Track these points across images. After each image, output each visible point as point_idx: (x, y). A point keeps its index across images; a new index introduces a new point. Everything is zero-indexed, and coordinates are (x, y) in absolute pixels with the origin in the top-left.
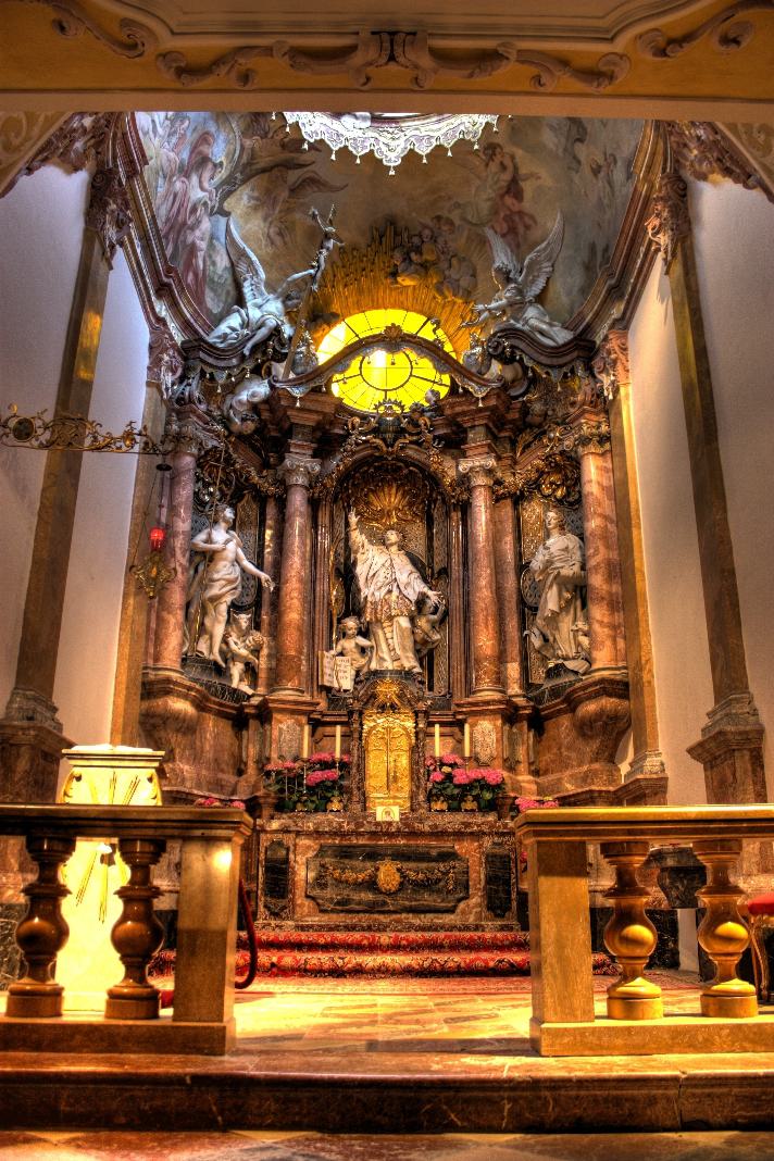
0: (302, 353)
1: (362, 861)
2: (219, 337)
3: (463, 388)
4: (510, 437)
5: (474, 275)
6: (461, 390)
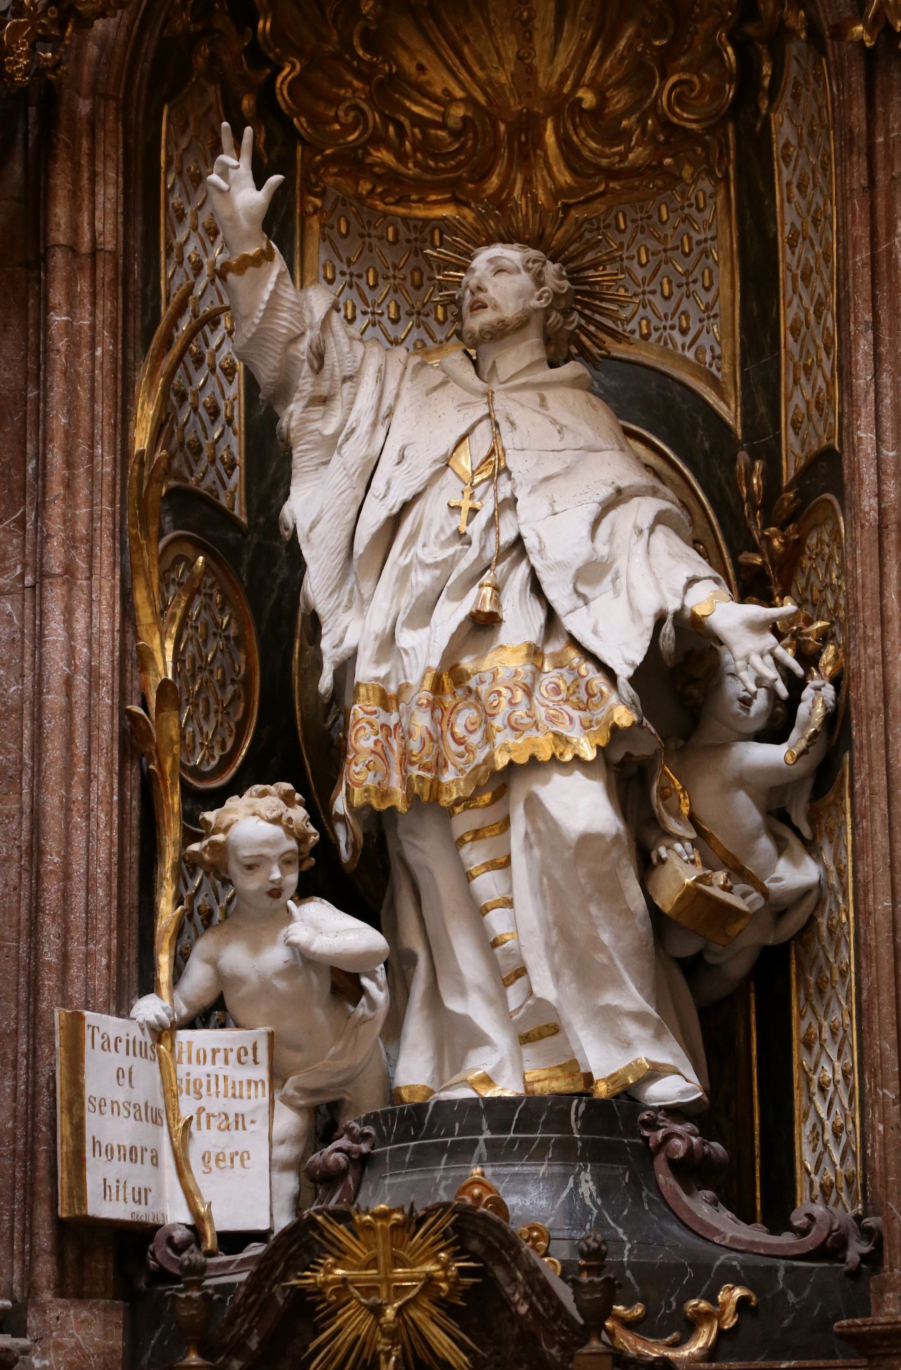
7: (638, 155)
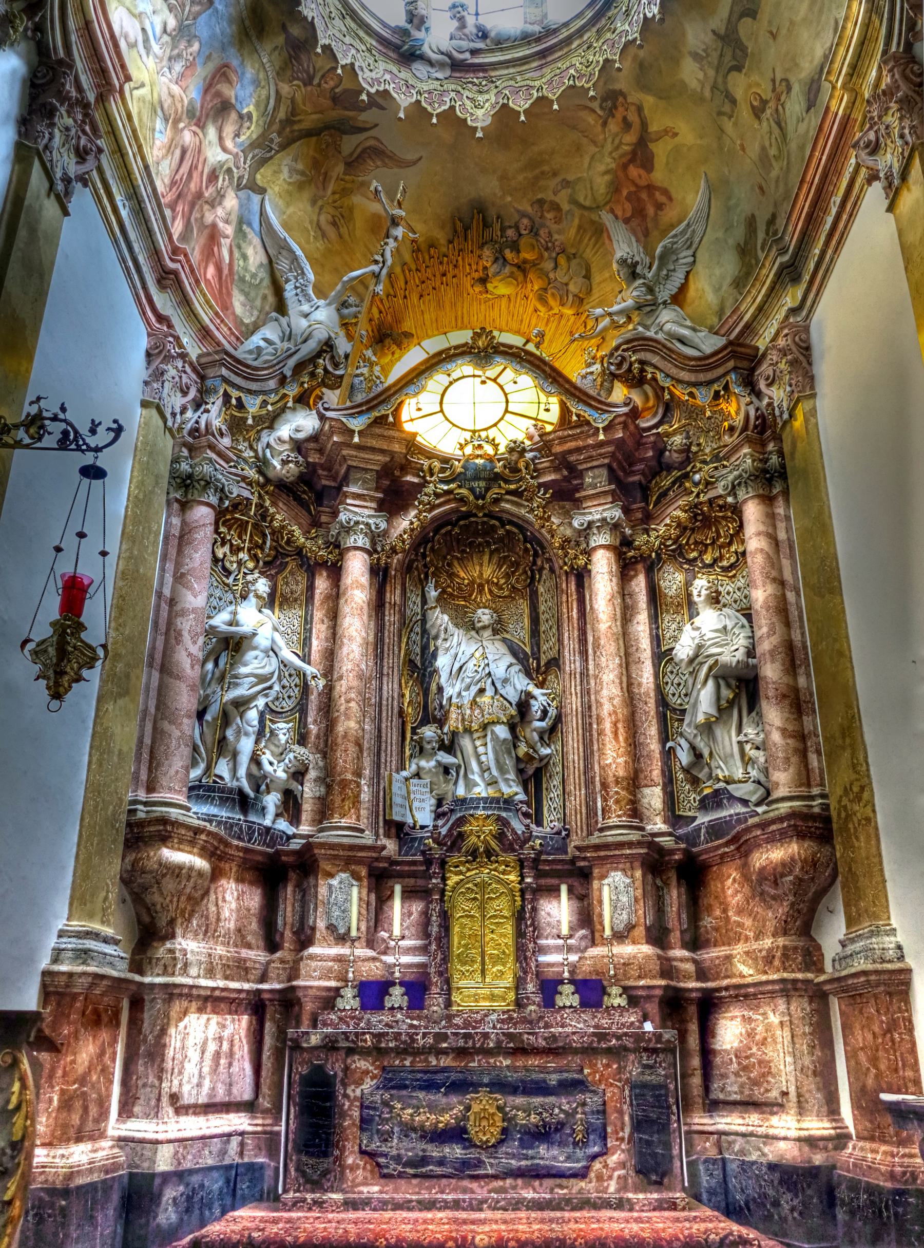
0: (362, 375)
1: (445, 1094)
2: (250, 352)
3: (578, 416)
4: (640, 483)
5: (588, 277)
6: (574, 418)
7: (506, 593)
